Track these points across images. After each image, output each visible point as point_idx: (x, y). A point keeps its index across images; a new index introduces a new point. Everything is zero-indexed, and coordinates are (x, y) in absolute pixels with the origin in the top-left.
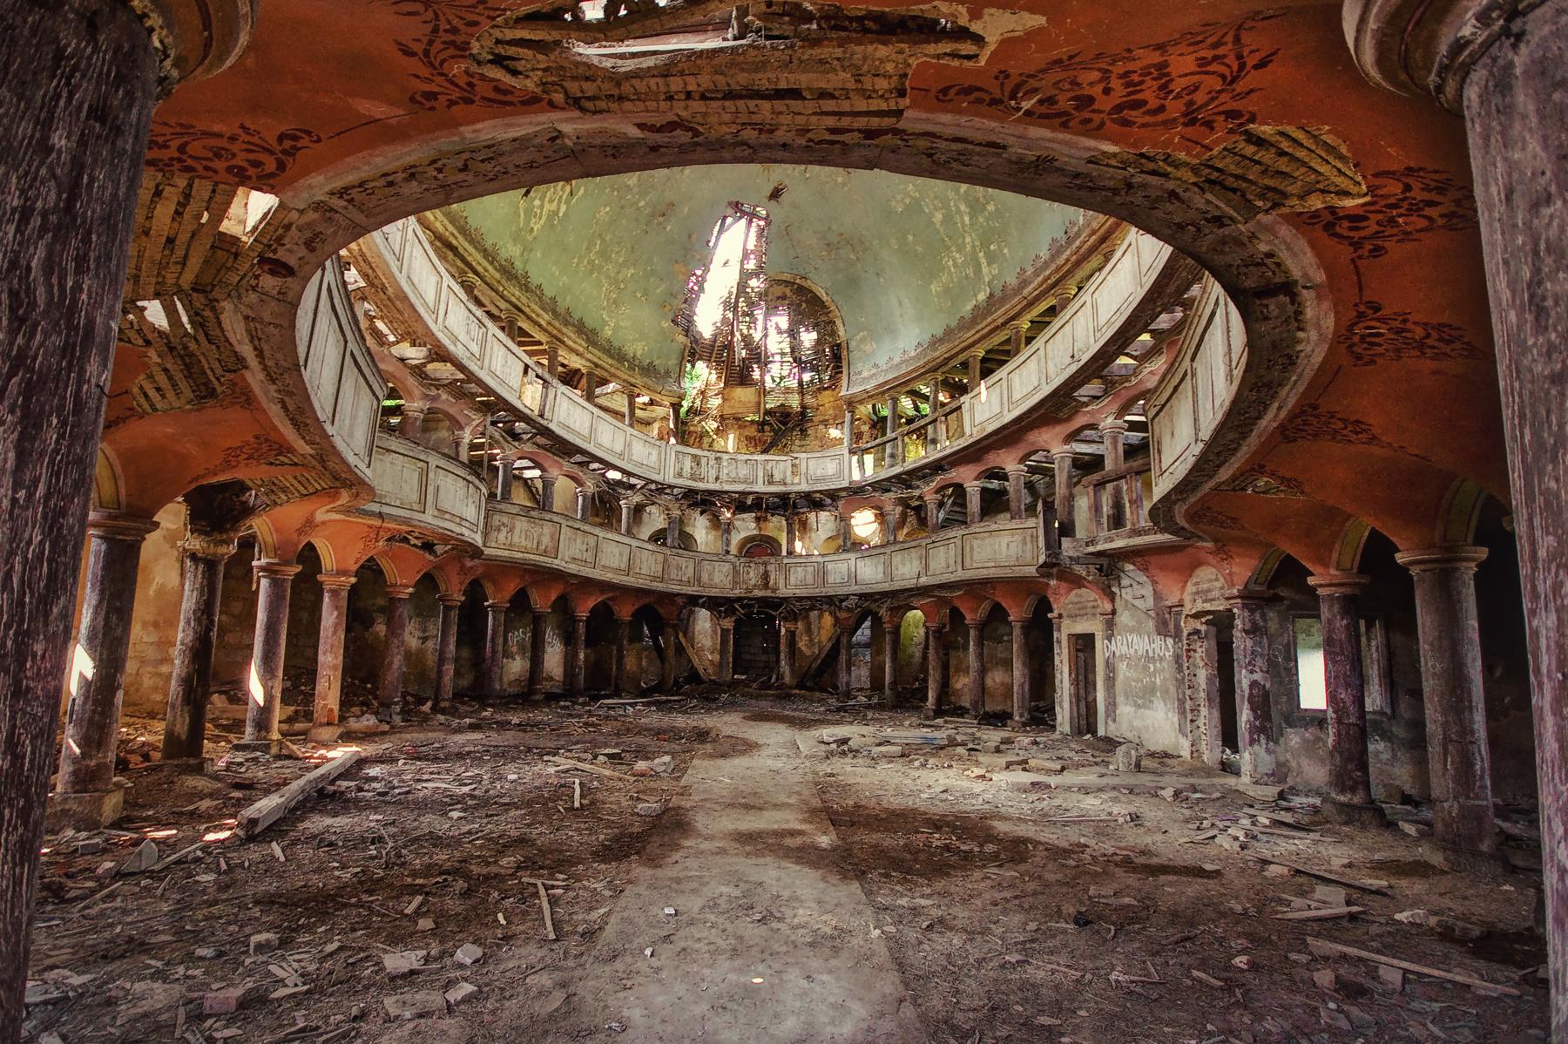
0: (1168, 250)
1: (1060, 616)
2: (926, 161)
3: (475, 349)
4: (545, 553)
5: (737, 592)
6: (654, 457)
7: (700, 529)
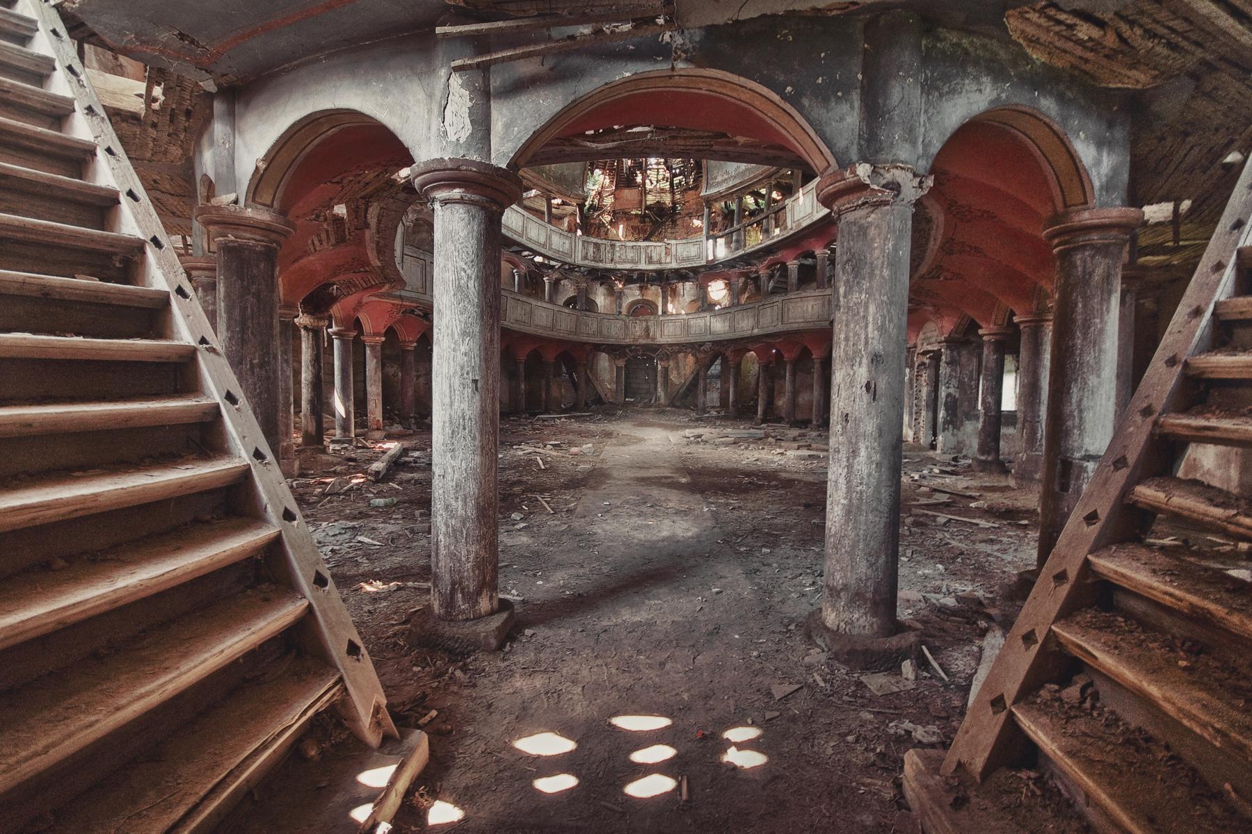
5: (628, 341)
6: (567, 246)
7: (601, 299)
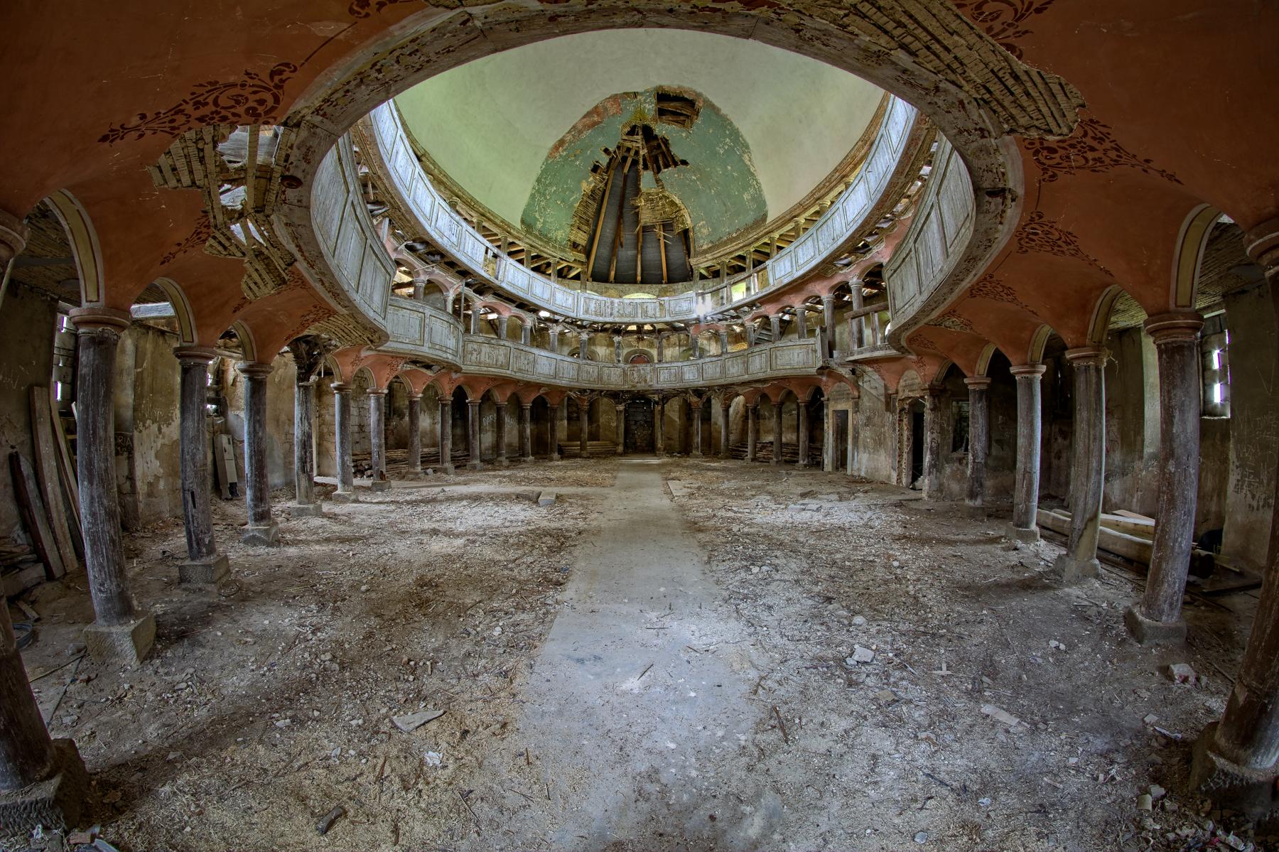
3: (454, 239)
4: (501, 367)
5: (626, 387)
6: (570, 301)
7: (602, 351)
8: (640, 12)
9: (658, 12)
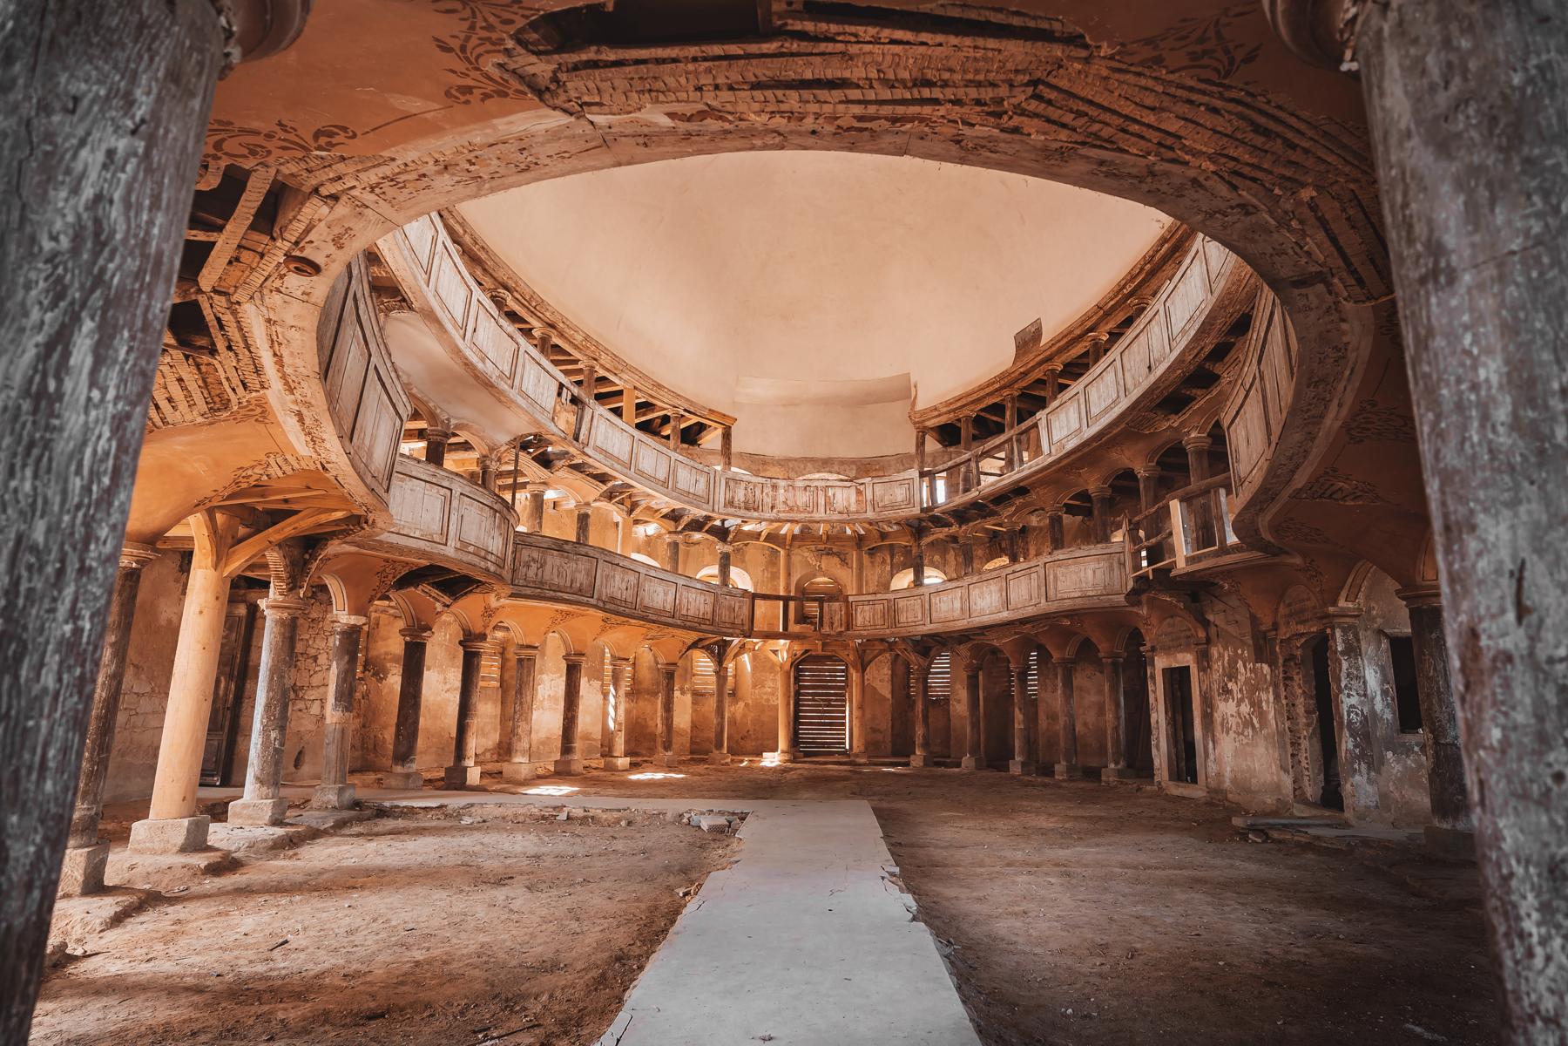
0: (1167, 220)
1: (1153, 649)
2: (954, 148)
6: (702, 485)
8: (780, 134)
9: (799, 134)
